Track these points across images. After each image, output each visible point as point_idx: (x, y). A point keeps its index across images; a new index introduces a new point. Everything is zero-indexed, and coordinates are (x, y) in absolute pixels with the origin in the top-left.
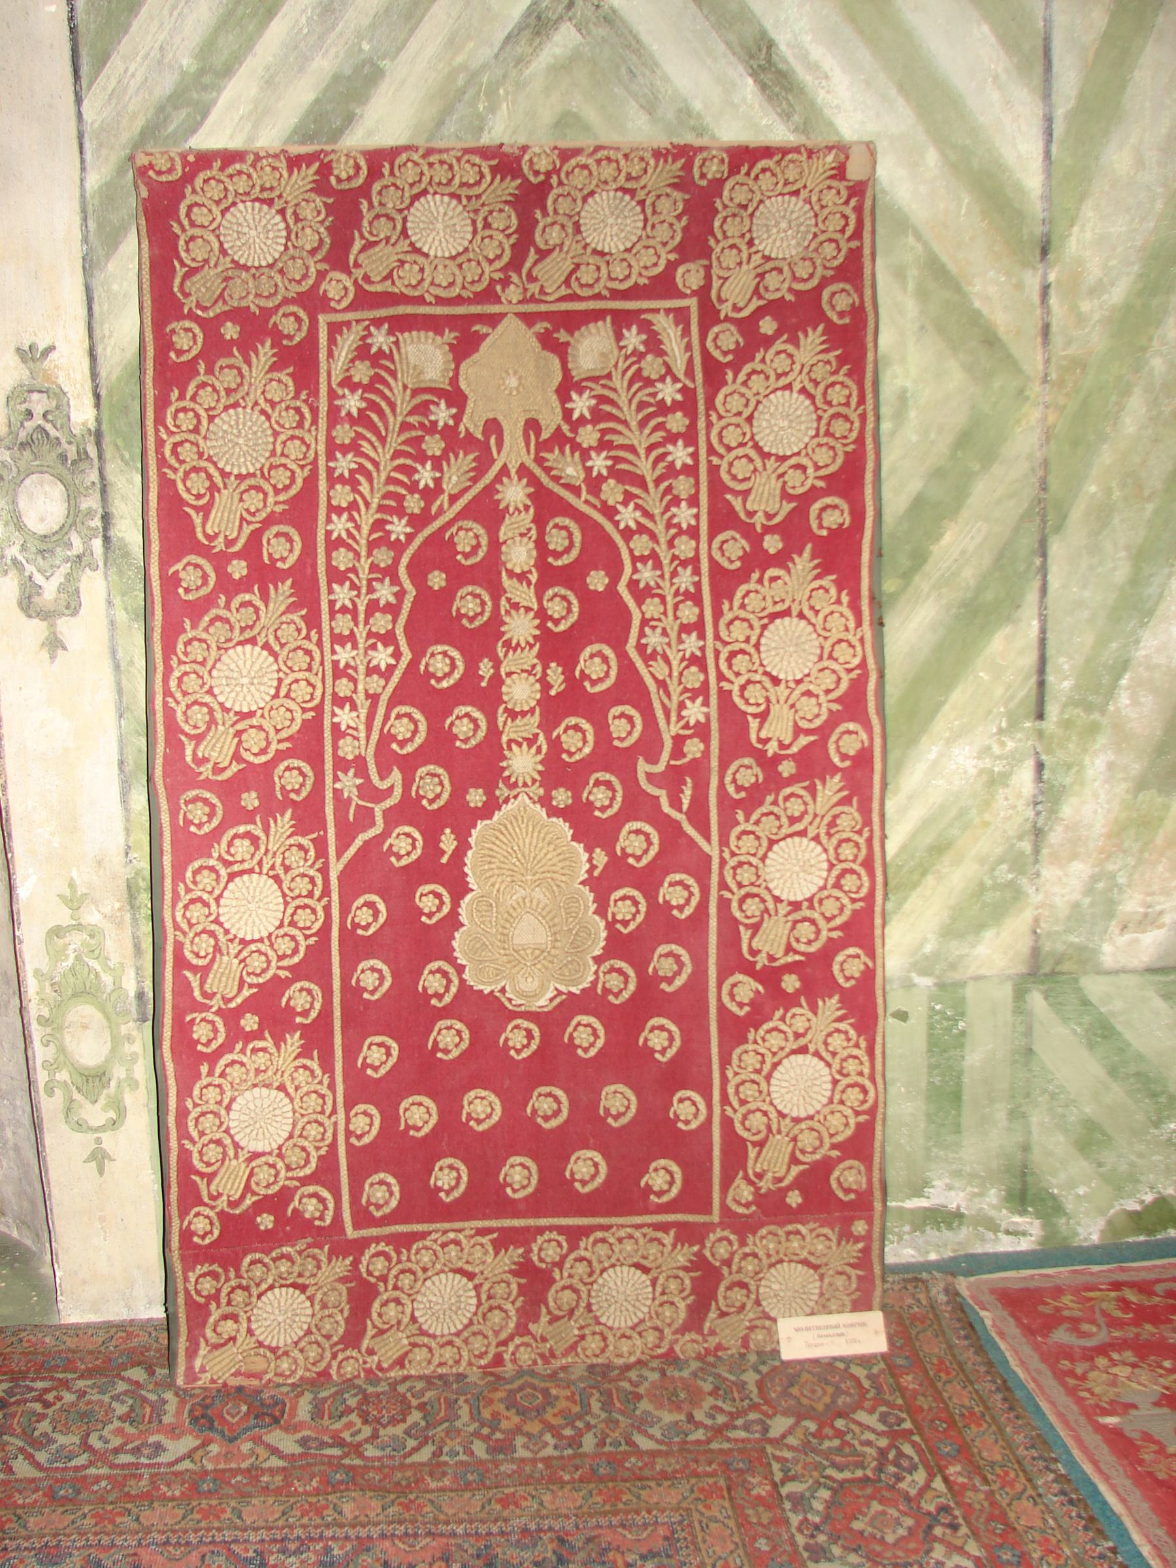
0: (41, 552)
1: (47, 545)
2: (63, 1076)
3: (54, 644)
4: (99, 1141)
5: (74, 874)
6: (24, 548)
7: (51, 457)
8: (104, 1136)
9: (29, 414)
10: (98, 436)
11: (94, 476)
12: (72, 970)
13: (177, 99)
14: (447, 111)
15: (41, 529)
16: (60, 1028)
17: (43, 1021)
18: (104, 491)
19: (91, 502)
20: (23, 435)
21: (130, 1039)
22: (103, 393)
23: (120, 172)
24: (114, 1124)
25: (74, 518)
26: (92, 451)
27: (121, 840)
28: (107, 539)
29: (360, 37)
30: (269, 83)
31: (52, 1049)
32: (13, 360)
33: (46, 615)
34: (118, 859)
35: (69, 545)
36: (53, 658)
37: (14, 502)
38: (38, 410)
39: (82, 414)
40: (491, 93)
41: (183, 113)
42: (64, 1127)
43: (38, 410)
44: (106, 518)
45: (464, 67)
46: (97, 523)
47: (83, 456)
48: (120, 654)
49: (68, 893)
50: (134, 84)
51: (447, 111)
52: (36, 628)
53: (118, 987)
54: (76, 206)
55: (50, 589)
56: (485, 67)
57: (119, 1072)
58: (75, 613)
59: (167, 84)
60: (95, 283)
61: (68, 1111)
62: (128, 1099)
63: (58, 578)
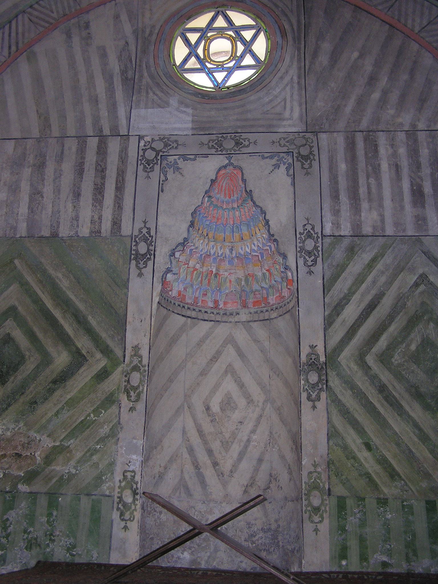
0: (312, 387)
1: (314, 386)
2: (309, 508)
3: (314, 407)
4: (317, 526)
5: (316, 459)
6: (308, 386)
7: (315, 368)
8: (318, 525)
9: (311, 359)
10: (326, 364)
11: (324, 372)
12: (313, 482)
13: (344, 298)
14: (399, 301)
15: (312, 383)
16: (309, 497)
17: (305, 494)
18: (326, 375)
19: (324, 377)
20: (310, 363)
21: (326, 500)
22: (327, 355)
23: (332, 311)
24: (321, 522)
25: (320, 380)
26: (324, 367)
27: (327, 452)
28: (327, 386)
29: (381, 287)
30: (362, 295)
31: (307, 501)
32: (308, 348)
33: (312, 401)
34: (326, 456)
35: (319, 386)
36: (314, 410)
37: (307, 377)
38: (313, 358)
39: (322, 359)
40: (408, 297)
41: (345, 301)
42: (308, 522)
43: (313, 358)
44: (327, 381)
45: (402, 293)
46: (325, 382)
47: (322, 367)
48: (329, 410)
49: (314, 463)
50: (335, 295)
51: (399, 301)
52: (311, 403)
53: (324, 487)
54: (323, 317)
55: (314, 395)
56: (406, 293)
57: (323, 508)
58: (319, 401)
59: (342, 296)
60: (326, 333)
61: (310, 518)
62: (324, 515)
63: (316, 393)
